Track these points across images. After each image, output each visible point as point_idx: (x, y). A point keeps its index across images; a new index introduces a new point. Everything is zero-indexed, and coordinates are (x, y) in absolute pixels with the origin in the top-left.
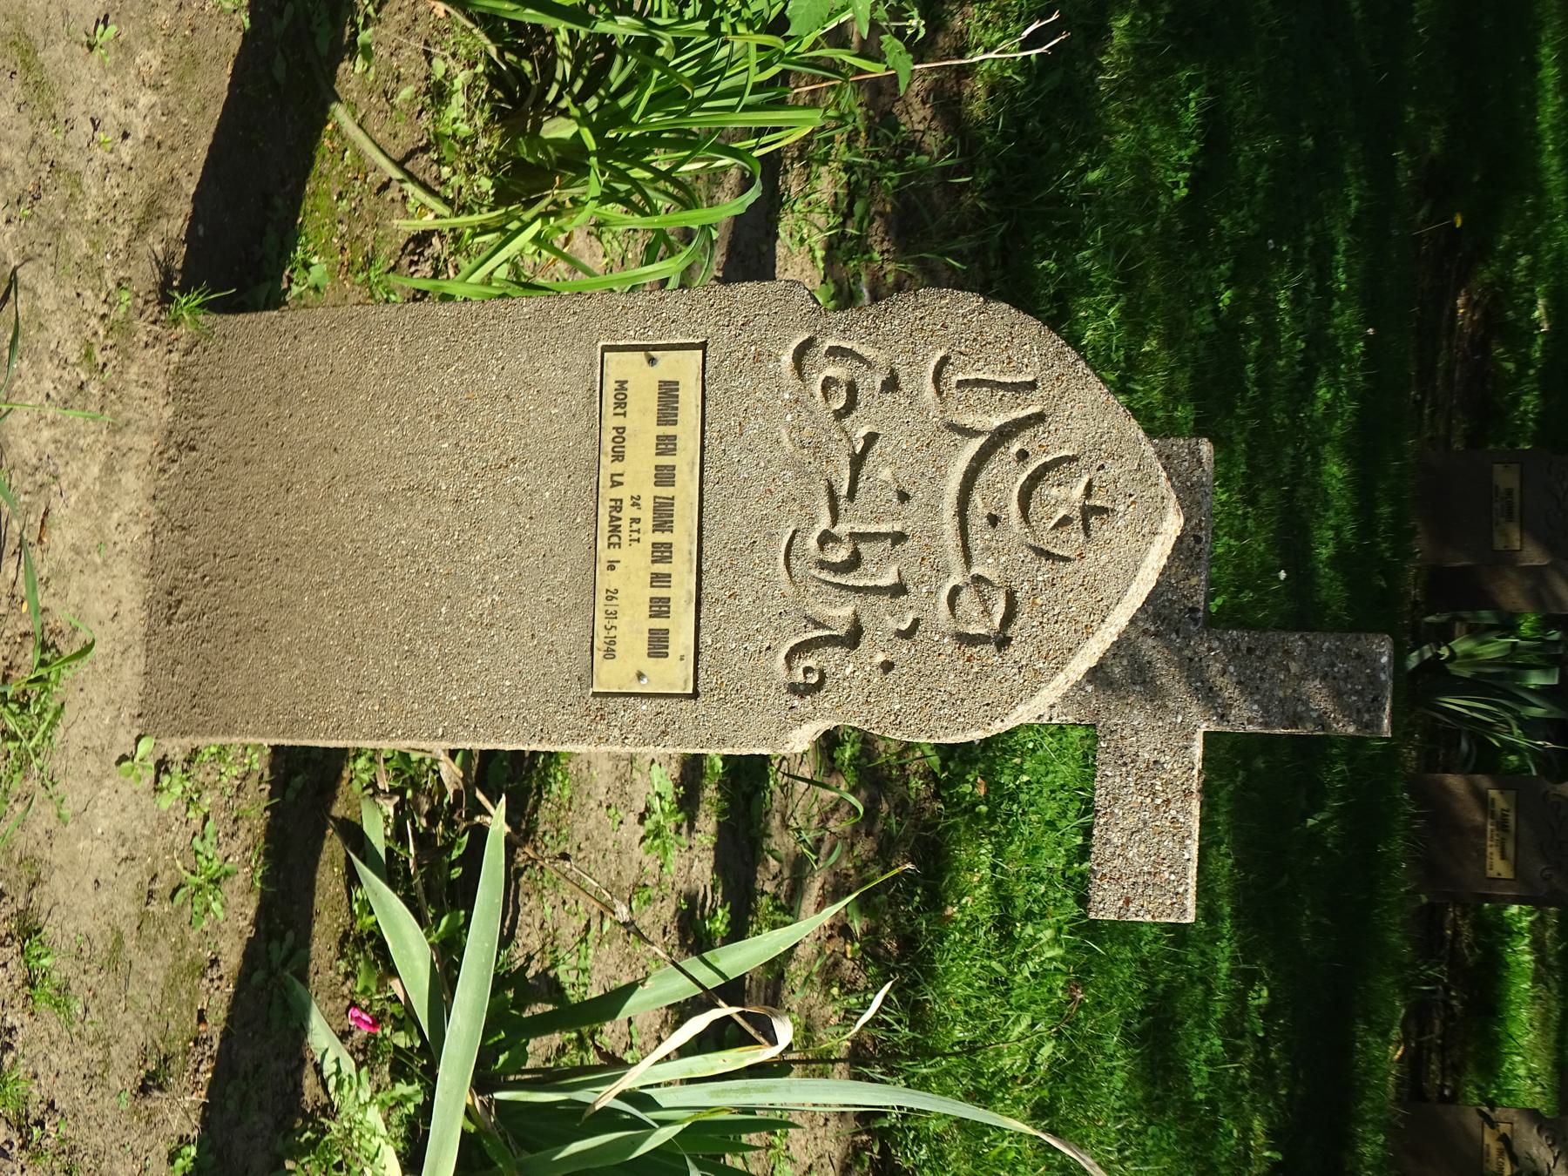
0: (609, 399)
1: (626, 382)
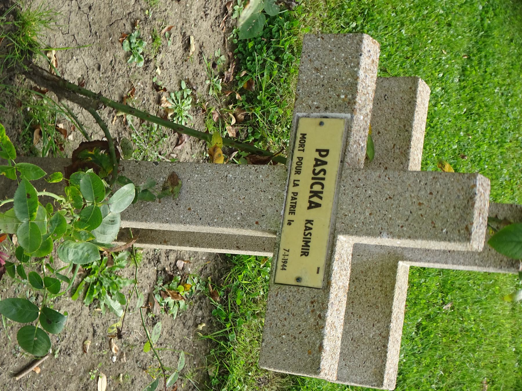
0: (297, 143)
1: (306, 134)
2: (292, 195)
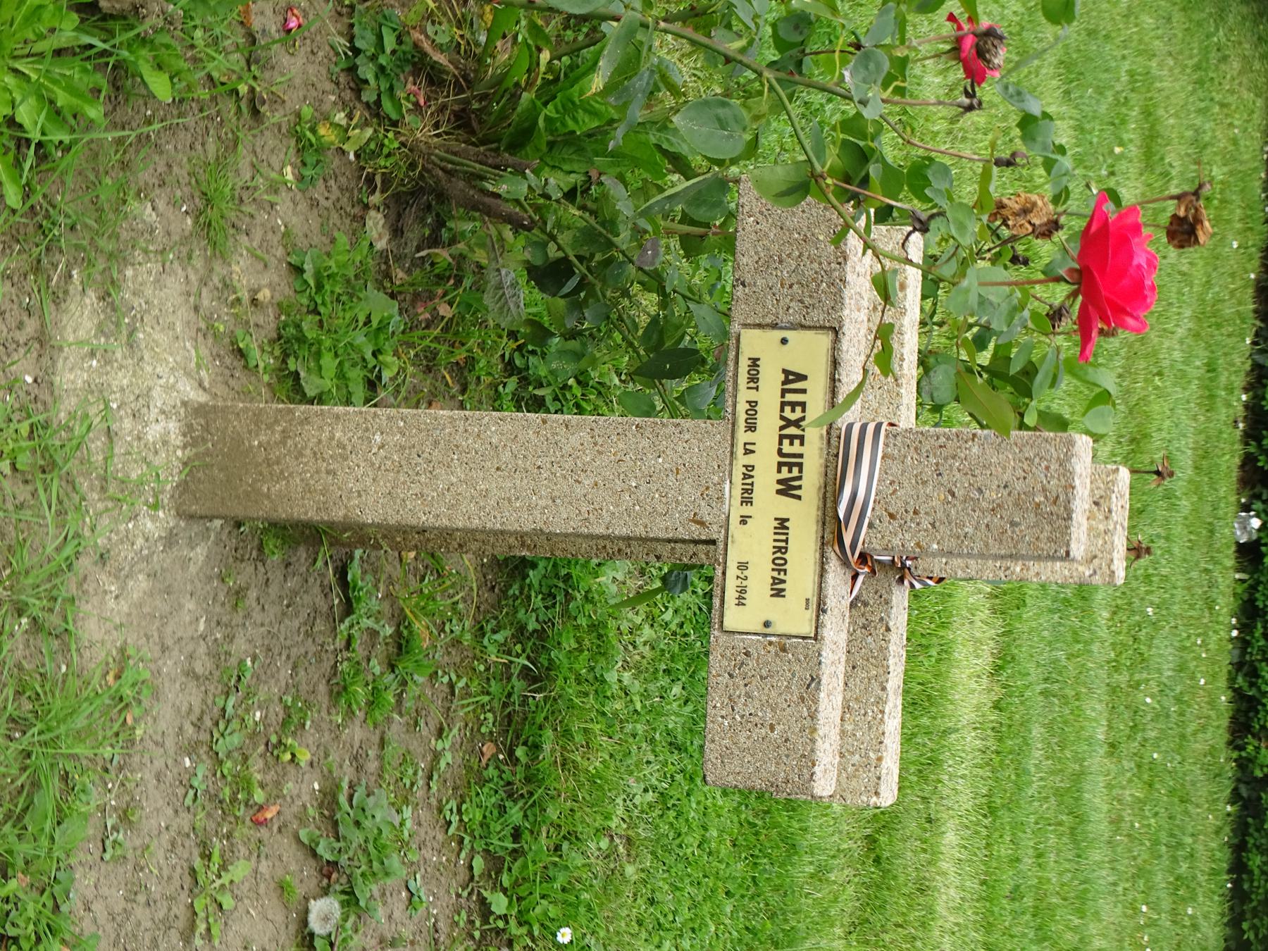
2: (744, 470)
